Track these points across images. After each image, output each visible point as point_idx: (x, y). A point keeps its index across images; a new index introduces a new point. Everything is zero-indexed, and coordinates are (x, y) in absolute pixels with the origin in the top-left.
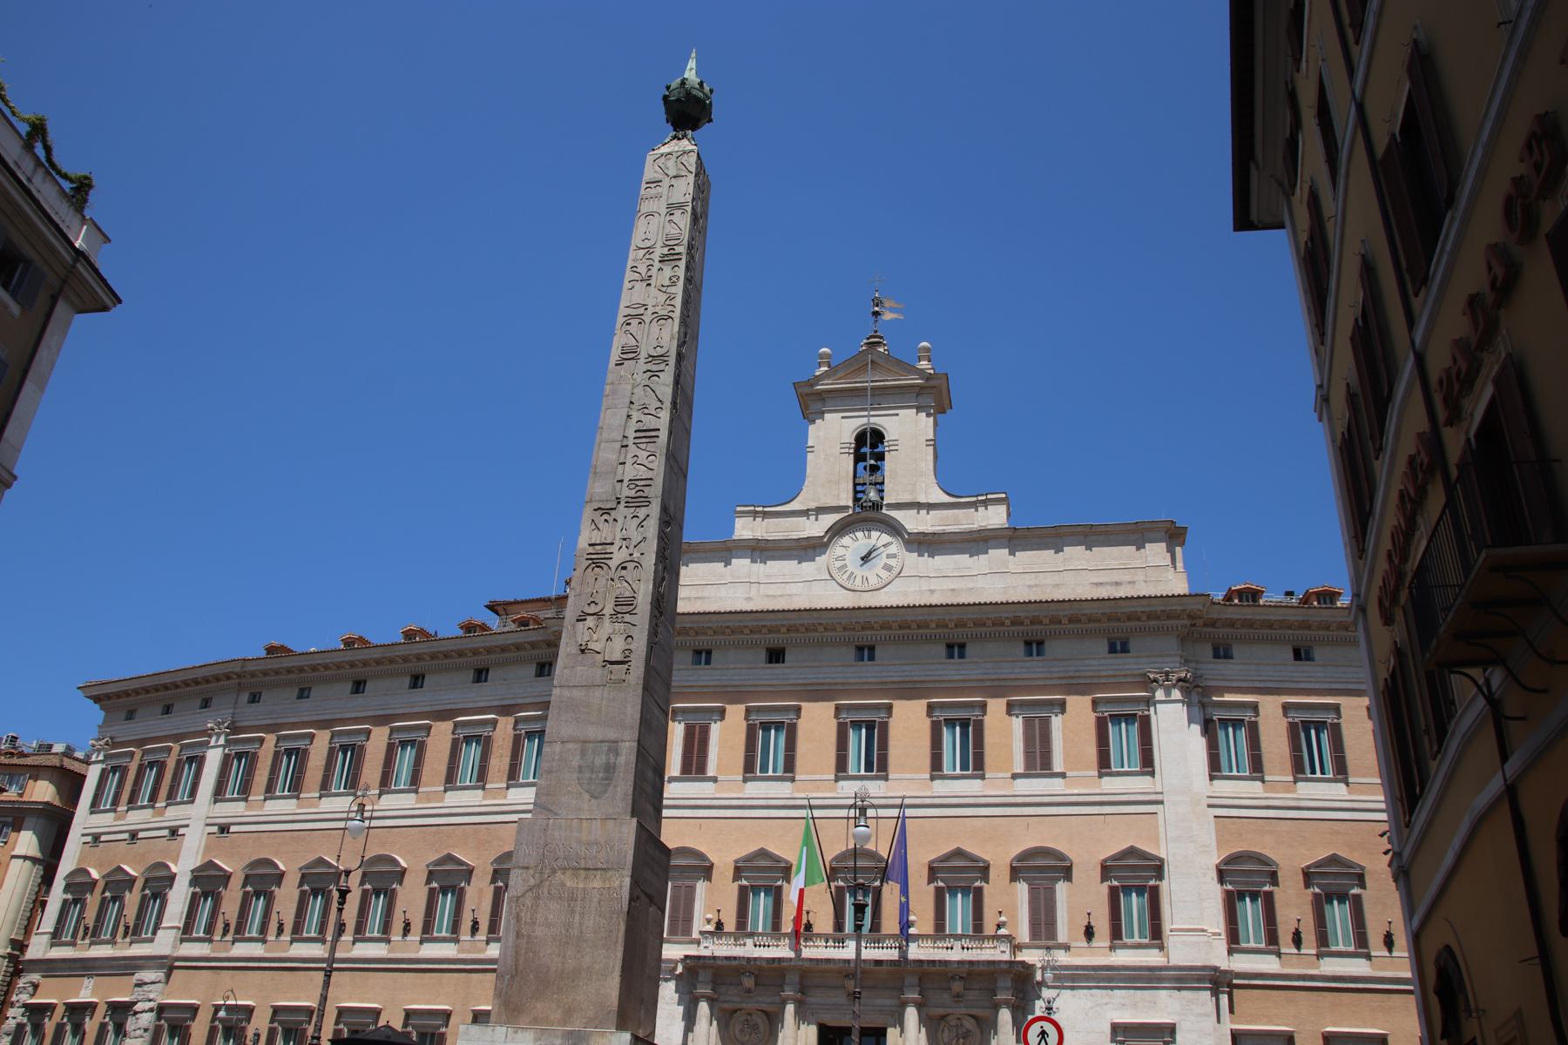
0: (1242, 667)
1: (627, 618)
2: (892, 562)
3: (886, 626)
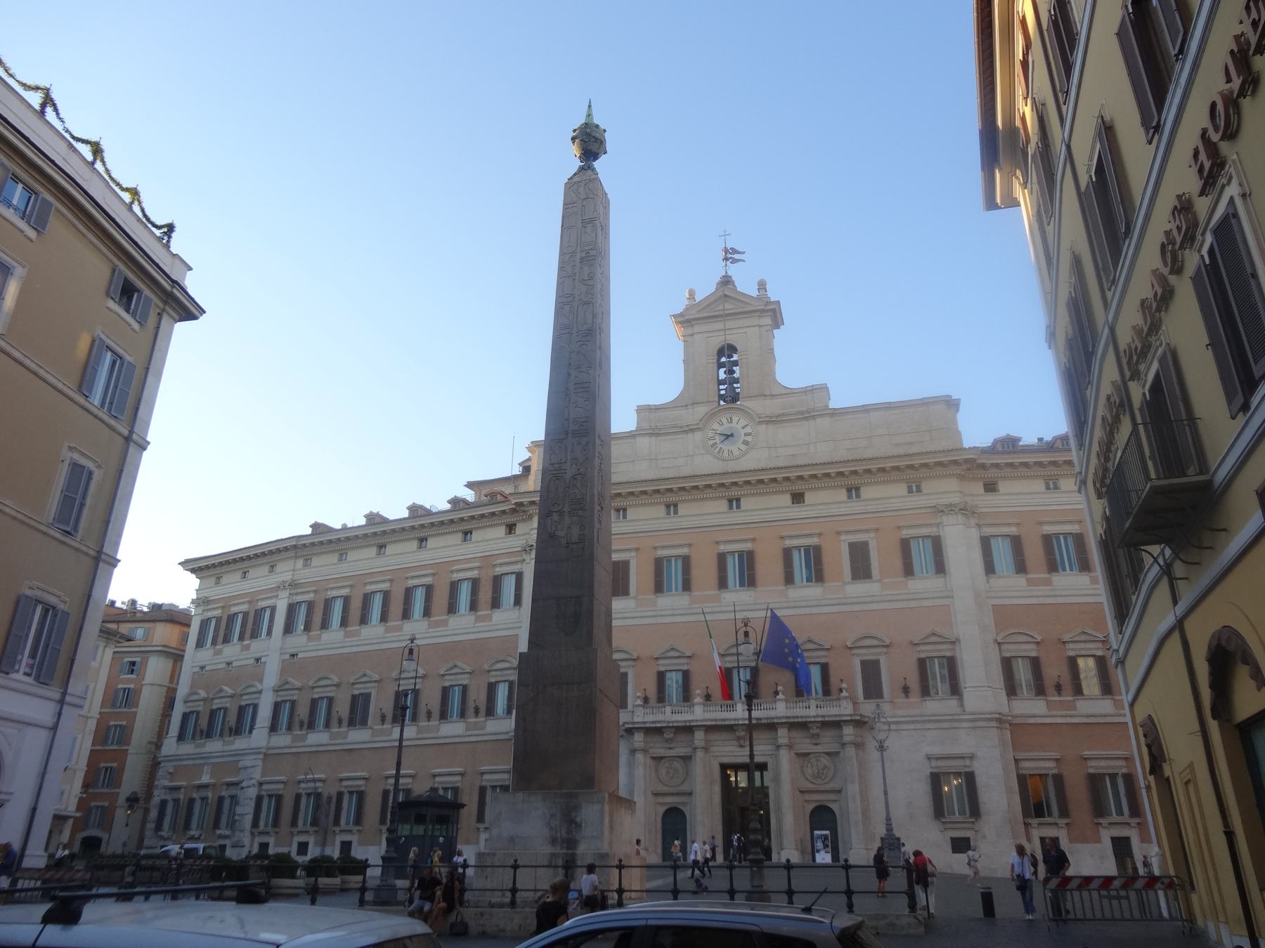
1: (580, 513)
2: (749, 439)
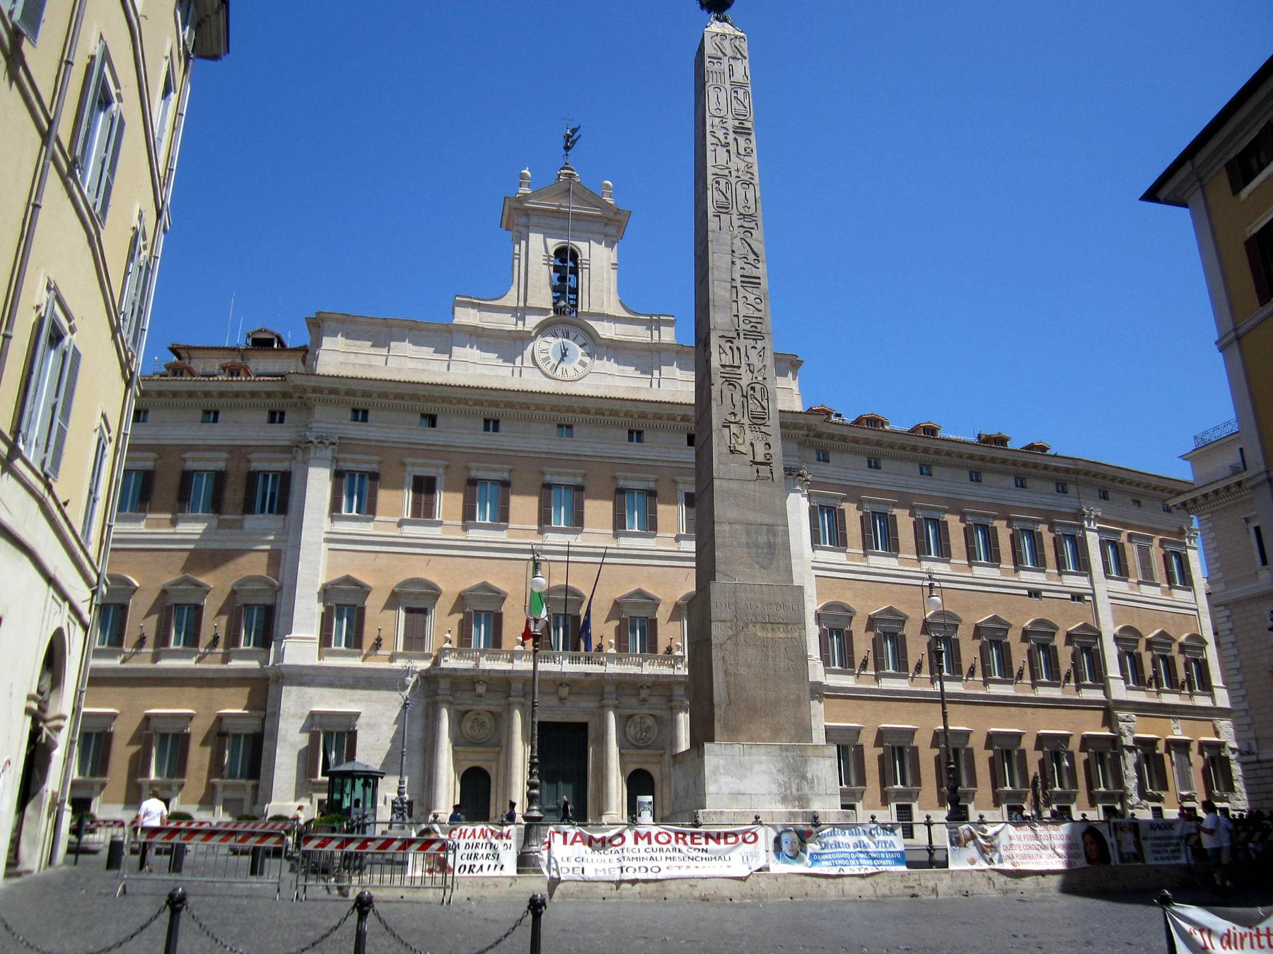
0: (835, 469)
1: (763, 429)
3: (585, 411)
